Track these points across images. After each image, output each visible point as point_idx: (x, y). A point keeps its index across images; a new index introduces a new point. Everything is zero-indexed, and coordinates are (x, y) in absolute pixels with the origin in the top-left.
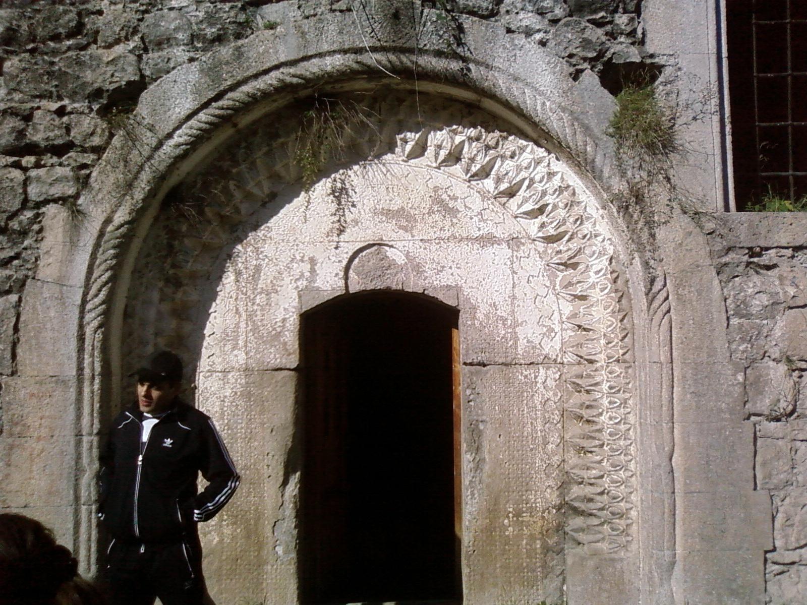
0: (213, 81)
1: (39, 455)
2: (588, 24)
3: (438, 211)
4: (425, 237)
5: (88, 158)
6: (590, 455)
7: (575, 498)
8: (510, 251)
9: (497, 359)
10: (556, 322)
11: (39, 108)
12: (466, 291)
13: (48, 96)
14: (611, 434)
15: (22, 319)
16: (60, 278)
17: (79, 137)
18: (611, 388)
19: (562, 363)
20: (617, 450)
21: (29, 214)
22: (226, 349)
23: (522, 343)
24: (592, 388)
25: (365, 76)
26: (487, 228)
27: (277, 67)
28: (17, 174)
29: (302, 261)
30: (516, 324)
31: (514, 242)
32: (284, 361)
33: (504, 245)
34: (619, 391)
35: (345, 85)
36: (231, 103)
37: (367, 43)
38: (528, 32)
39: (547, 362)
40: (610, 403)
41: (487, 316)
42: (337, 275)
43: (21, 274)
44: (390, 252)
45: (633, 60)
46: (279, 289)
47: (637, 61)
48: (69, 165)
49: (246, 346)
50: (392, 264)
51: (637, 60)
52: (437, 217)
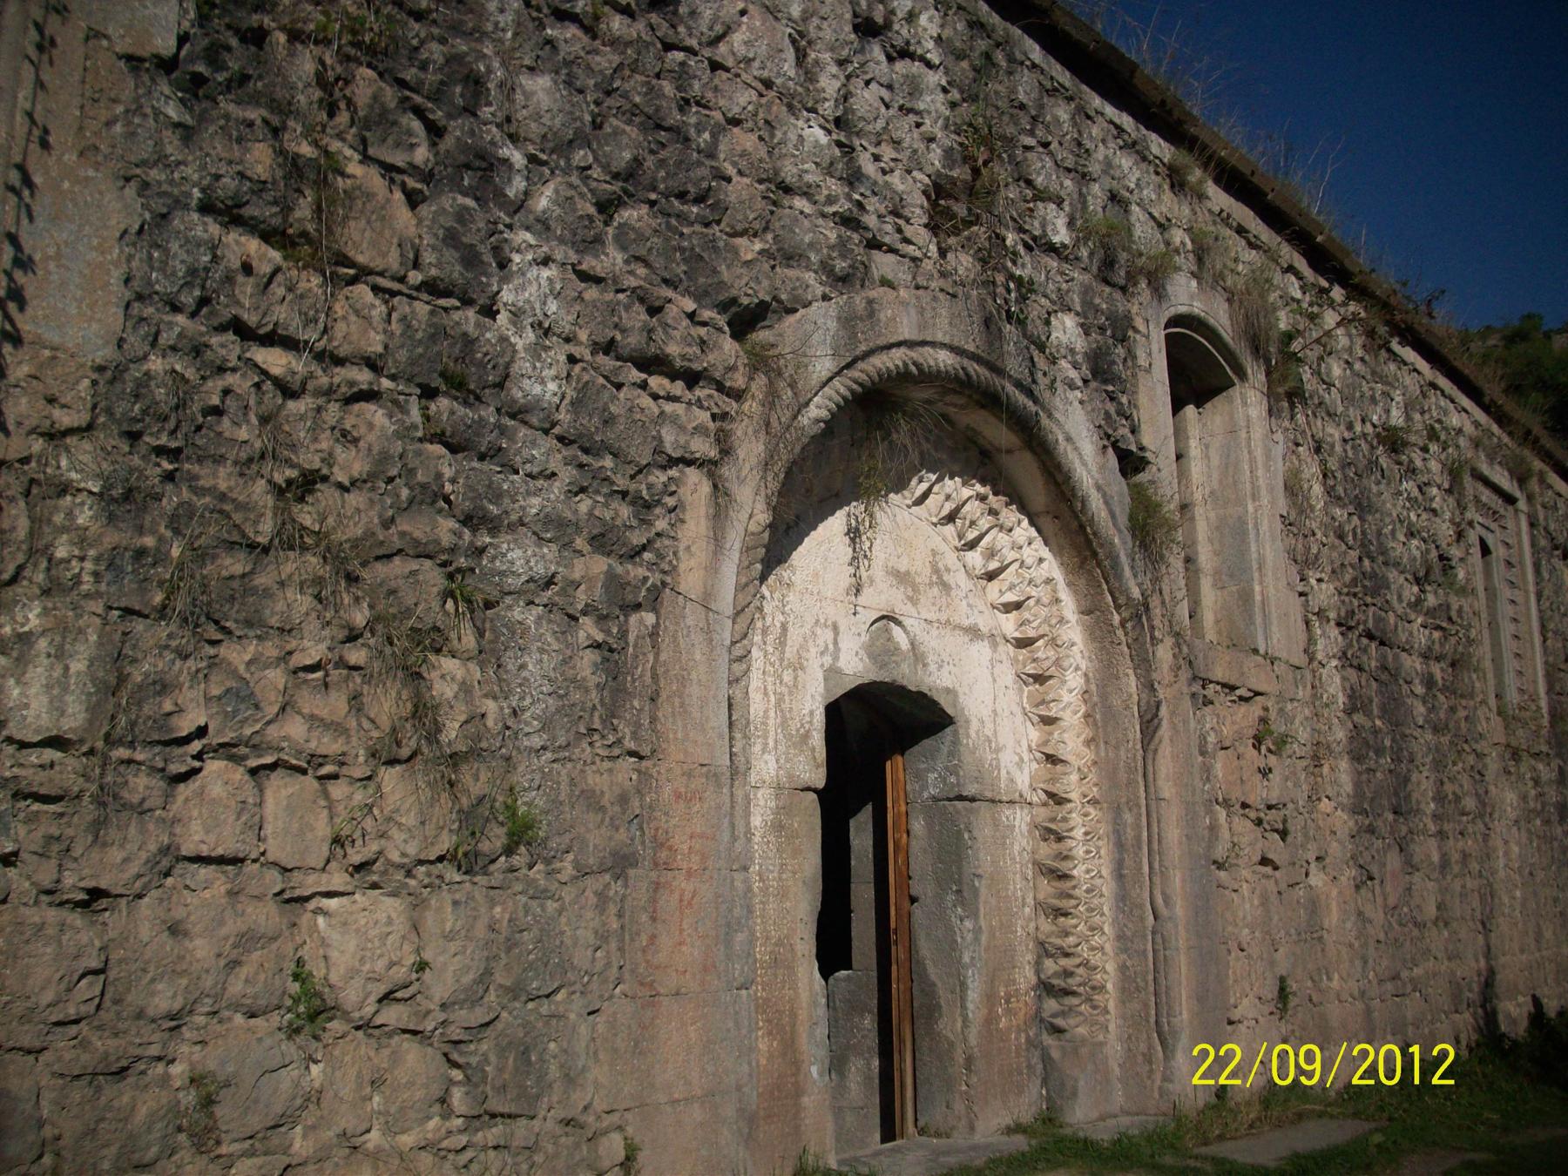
1: (690, 904)
5: (731, 406)
6: (1062, 919)
11: (670, 301)
14: (1088, 891)
21: (659, 478)
23: (1003, 772)
27: (899, 344)
28: (646, 401)
30: (998, 750)
37: (971, 347)
43: (654, 578)
44: (897, 631)
50: (897, 649)
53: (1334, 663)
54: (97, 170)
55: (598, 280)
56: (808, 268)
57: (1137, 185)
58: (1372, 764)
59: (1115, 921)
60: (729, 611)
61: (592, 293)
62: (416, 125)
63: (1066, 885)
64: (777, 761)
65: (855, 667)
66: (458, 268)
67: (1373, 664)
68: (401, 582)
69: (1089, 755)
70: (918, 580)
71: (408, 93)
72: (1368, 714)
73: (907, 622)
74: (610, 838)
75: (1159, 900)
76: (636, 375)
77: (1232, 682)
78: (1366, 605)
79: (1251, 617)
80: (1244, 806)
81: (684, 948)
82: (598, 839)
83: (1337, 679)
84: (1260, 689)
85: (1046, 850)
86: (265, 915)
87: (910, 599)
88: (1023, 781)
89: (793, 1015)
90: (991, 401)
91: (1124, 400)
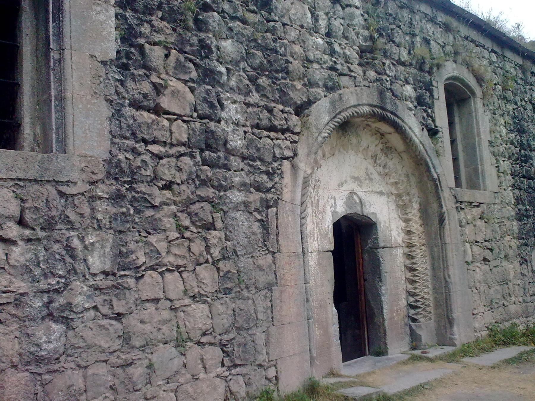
5: (296, 138)
11: (275, 107)
12: (378, 215)
21: (275, 165)
23: (393, 238)
30: (391, 231)
37: (375, 103)
38: (410, 109)
43: (276, 197)
44: (355, 197)
49: (317, 240)
53: (510, 188)
54: (97, 99)
55: (252, 105)
56: (319, 87)
57: (433, 33)
58: (526, 222)
59: (432, 283)
60: (300, 204)
61: (250, 109)
62: (191, 65)
65: (341, 210)
66: (208, 109)
67: (525, 187)
68: (198, 210)
70: (362, 179)
71: (187, 55)
72: (524, 204)
73: (359, 193)
74: (267, 279)
75: (447, 276)
76: (265, 133)
77: (471, 201)
78: (523, 167)
79: (478, 176)
80: (477, 242)
82: (262, 279)
83: (511, 195)
84: (481, 202)
85: (408, 262)
86: (166, 314)
88: (400, 240)
91: (429, 111)
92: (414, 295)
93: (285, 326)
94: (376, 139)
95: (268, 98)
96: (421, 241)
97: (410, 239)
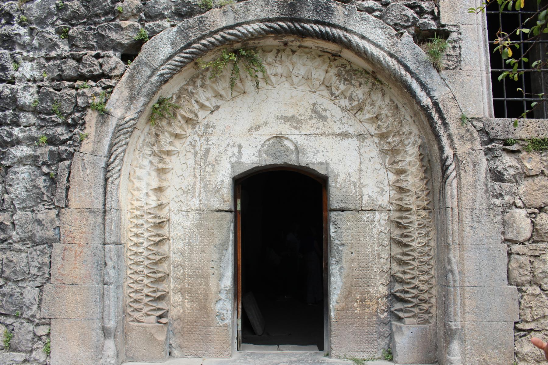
0: (184, 38)
2: (405, 7)
3: (315, 117)
4: (308, 133)
7: (397, 291)
8: (358, 142)
9: (350, 207)
10: (386, 185)
11: (86, 54)
12: (332, 166)
13: (91, 48)
15: (71, 175)
16: (93, 152)
17: (108, 71)
18: (419, 225)
19: (390, 210)
20: (423, 262)
22: (188, 198)
23: (365, 198)
24: (408, 225)
25: (273, 35)
26: (346, 128)
27: (222, 30)
29: (234, 146)
30: (362, 186)
31: (361, 137)
32: (222, 205)
33: (355, 139)
34: (424, 226)
35: (261, 41)
36: (193, 50)
37: (275, 15)
38: (370, 10)
39: (381, 209)
40: (419, 234)
41: (344, 180)
42: (254, 154)
43: (71, 149)
44: (286, 142)
45: (433, 28)
46: (219, 162)
47: (435, 28)
48: (101, 86)
49: (200, 196)
50: (287, 150)
51: (435, 28)
52: (314, 121)
63: (405, 250)
64: (200, 201)
69: (422, 184)
70: (300, 118)
76: (67, 83)
81: (76, 269)
85: (396, 233)
87: (295, 128)
88: (383, 201)
89: (206, 295)
90: (304, 34)
92: (402, 282)
93: (67, 286)
94: (324, 62)
95: (77, 46)
96: (419, 203)
97: (401, 199)
